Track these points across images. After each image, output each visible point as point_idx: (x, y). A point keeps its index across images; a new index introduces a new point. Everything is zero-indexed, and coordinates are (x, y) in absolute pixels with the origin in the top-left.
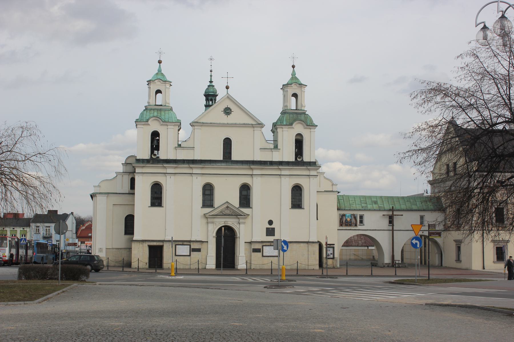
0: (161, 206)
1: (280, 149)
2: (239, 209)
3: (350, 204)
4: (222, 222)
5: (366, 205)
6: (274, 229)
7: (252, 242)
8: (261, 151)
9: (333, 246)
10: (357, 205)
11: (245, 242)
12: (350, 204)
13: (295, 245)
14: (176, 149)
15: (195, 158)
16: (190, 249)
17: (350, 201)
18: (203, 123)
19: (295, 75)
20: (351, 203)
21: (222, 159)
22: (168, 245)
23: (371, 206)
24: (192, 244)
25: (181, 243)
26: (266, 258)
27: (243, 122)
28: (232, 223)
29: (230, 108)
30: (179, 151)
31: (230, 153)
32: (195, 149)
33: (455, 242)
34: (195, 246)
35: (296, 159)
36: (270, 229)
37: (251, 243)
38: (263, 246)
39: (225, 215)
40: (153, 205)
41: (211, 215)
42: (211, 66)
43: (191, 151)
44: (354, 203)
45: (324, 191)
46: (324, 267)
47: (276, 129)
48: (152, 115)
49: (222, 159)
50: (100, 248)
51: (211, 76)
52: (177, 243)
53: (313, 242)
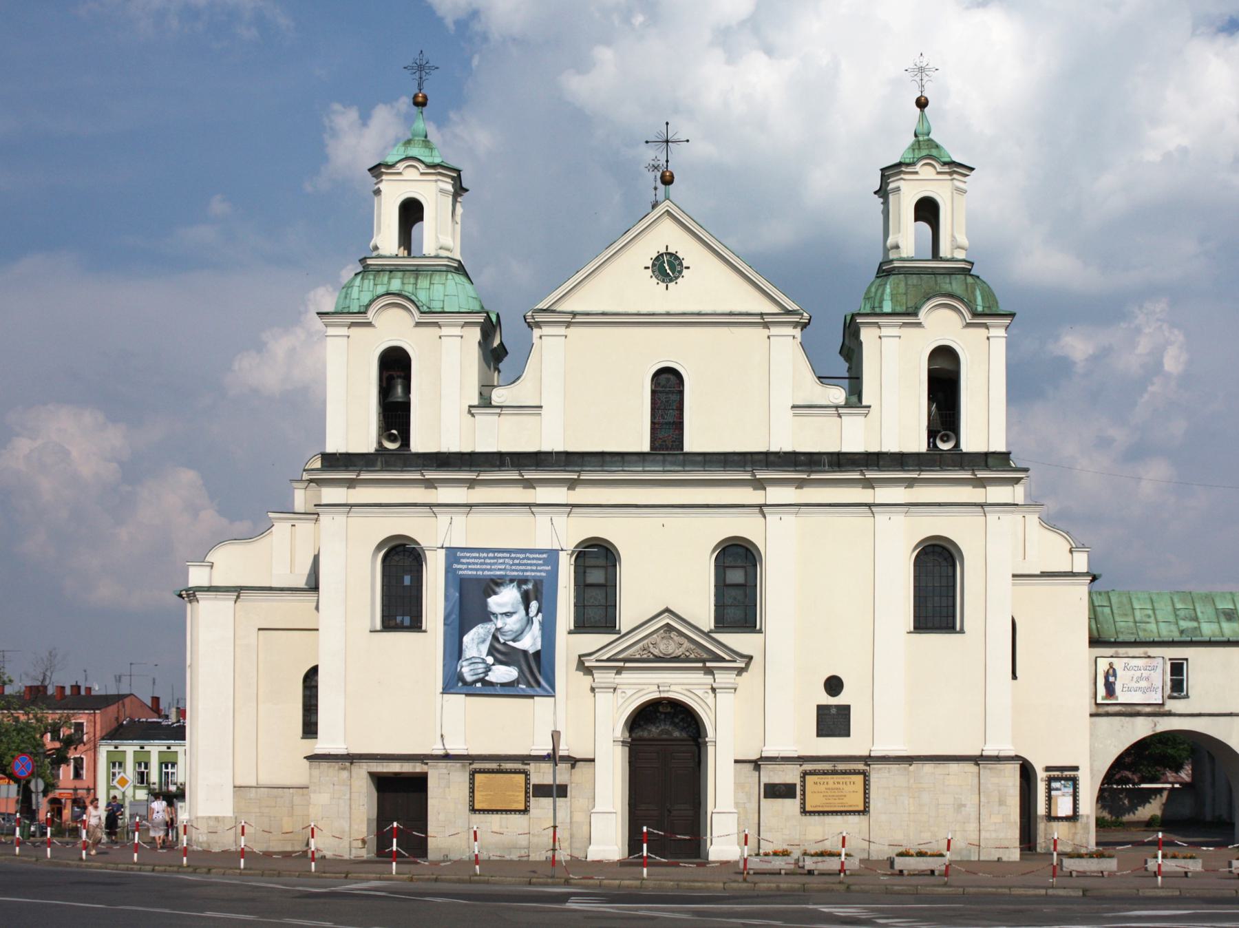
0: (421, 627)
1: (869, 407)
2: (714, 635)
3: (1135, 622)
5: (1195, 624)
6: (847, 708)
7: (762, 759)
9: (1072, 773)
10: (1162, 625)
11: (736, 761)
12: (1135, 622)
13: (928, 768)
15: (546, 448)
17: (1138, 613)
18: (574, 314)
20: (1138, 618)
21: (646, 447)
22: (445, 771)
23: (1215, 627)
24: (532, 767)
25: (494, 766)
26: (816, 818)
27: (727, 309)
30: (485, 420)
31: (678, 426)
32: (543, 411)
34: (542, 774)
35: (932, 444)
36: (833, 711)
37: (757, 764)
38: (805, 774)
39: (658, 659)
40: (389, 624)
41: (605, 658)
43: (528, 421)
44: (1149, 616)
45: (1038, 572)
46: (1038, 850)
47: (856, 334)
48: (381, 290)
49: (646, 447)
52: (477, 766)
53: (998, 759)
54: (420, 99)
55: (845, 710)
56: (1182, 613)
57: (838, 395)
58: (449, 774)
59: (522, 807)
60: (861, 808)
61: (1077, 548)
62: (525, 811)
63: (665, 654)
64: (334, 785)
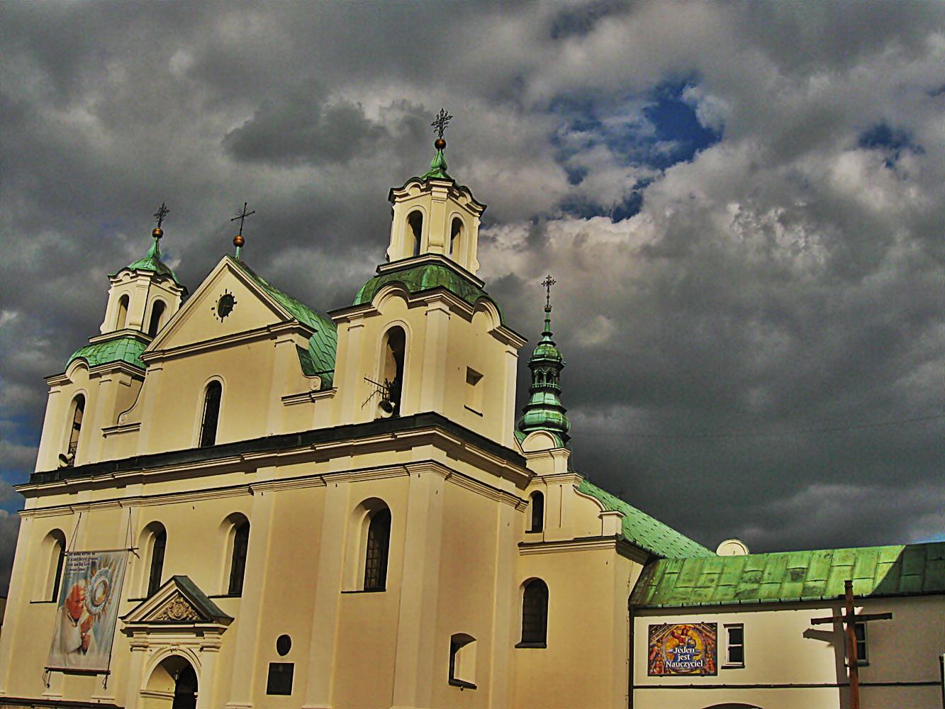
36: (281, 669)
41: (137, 620)
54: (157, 232)
56: (747, 576)
57: (316, 383)
61: (606, 511)
63: (177, 617)
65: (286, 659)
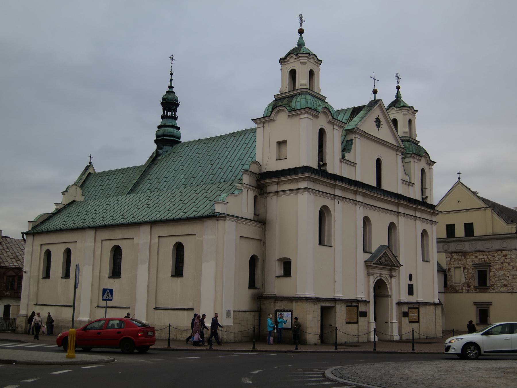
4: (378, 273)
8: (402, 183)
14: (341, 162)
16: (357, 313)
19: (401, 98)
28: (386, 277)
29: (380, 119)
32: (357, 166)
33: (475, 304)
38: (410, 308)
42: (172, 67)
50: (229, 311)
51: (171, 80)
55: (412, 285)
58: (341, 307)
59: (356, 321)
60: (417, 321)
62: (357, 322)
64: (313, 311)
65: (412, 283)
